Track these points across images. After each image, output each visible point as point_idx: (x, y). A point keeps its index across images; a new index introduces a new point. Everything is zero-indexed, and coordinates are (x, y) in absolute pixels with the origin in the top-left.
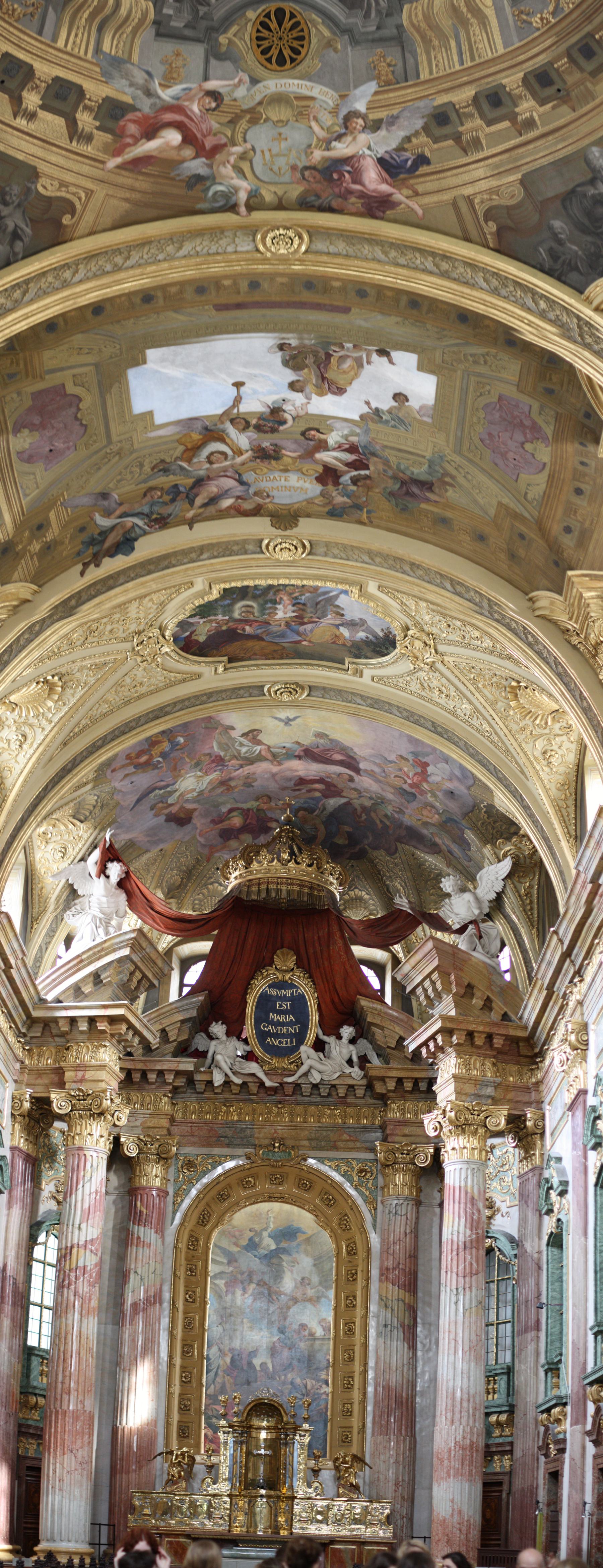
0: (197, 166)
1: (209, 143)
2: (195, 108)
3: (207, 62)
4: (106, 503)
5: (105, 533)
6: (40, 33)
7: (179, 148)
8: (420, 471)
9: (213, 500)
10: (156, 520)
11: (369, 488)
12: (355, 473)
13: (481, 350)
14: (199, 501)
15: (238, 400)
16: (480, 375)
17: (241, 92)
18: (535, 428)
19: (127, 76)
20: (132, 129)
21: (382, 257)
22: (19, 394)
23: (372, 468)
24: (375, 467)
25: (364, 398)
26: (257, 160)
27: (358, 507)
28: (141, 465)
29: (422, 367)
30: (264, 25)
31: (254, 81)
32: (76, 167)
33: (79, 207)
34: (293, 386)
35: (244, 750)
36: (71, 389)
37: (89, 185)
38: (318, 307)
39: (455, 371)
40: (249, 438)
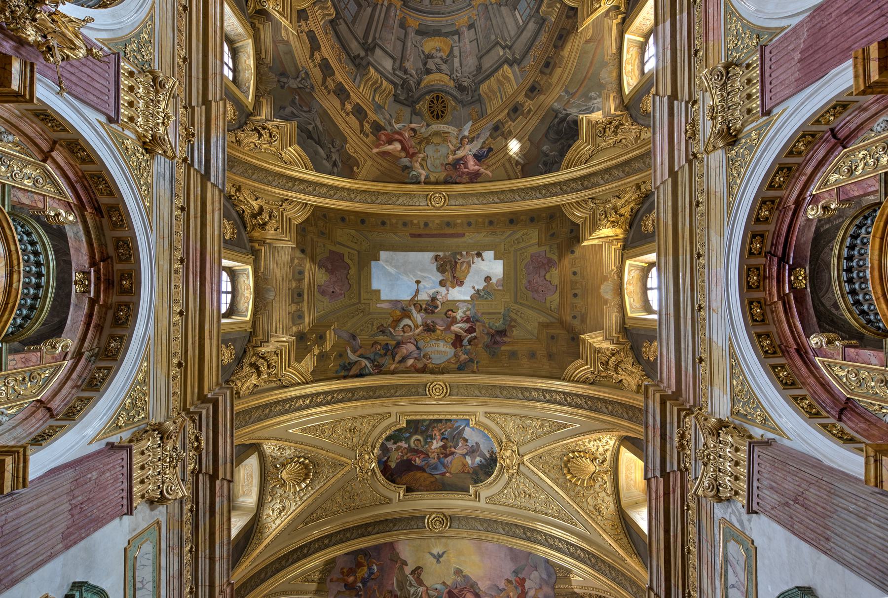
0: (406, 161)
1: (411, 152)
2: (407, 135)
3: (411, 115)
4: (354, 343)
5: (352, 364)
6: (354, 82)
7: (400, 151)
9: (404, 359)
10: (376, 366)
11: (476, 345)
12: (470, 336)
13: (520, 234)
14: (398, 358)
15: (417, 292)
16: (521, 249)
17: (423, 130)
21: (477, 202)
22: (324, 246)
23: (477, 330)
24: (479, 327)
25: (472, 285)
26: (429, 161)
27: (471, 360)
28: (373, 325)
29: (496, 258)
30: (432, 101)
31: (428, 125)
32: (362, 146)
33: (361, 165)
34: (442, 283)
35: (412, 590)
36: (346, 260)
37: (366, 158)
38: (452, 235)
39: (510, 253)
40: (421, 316)
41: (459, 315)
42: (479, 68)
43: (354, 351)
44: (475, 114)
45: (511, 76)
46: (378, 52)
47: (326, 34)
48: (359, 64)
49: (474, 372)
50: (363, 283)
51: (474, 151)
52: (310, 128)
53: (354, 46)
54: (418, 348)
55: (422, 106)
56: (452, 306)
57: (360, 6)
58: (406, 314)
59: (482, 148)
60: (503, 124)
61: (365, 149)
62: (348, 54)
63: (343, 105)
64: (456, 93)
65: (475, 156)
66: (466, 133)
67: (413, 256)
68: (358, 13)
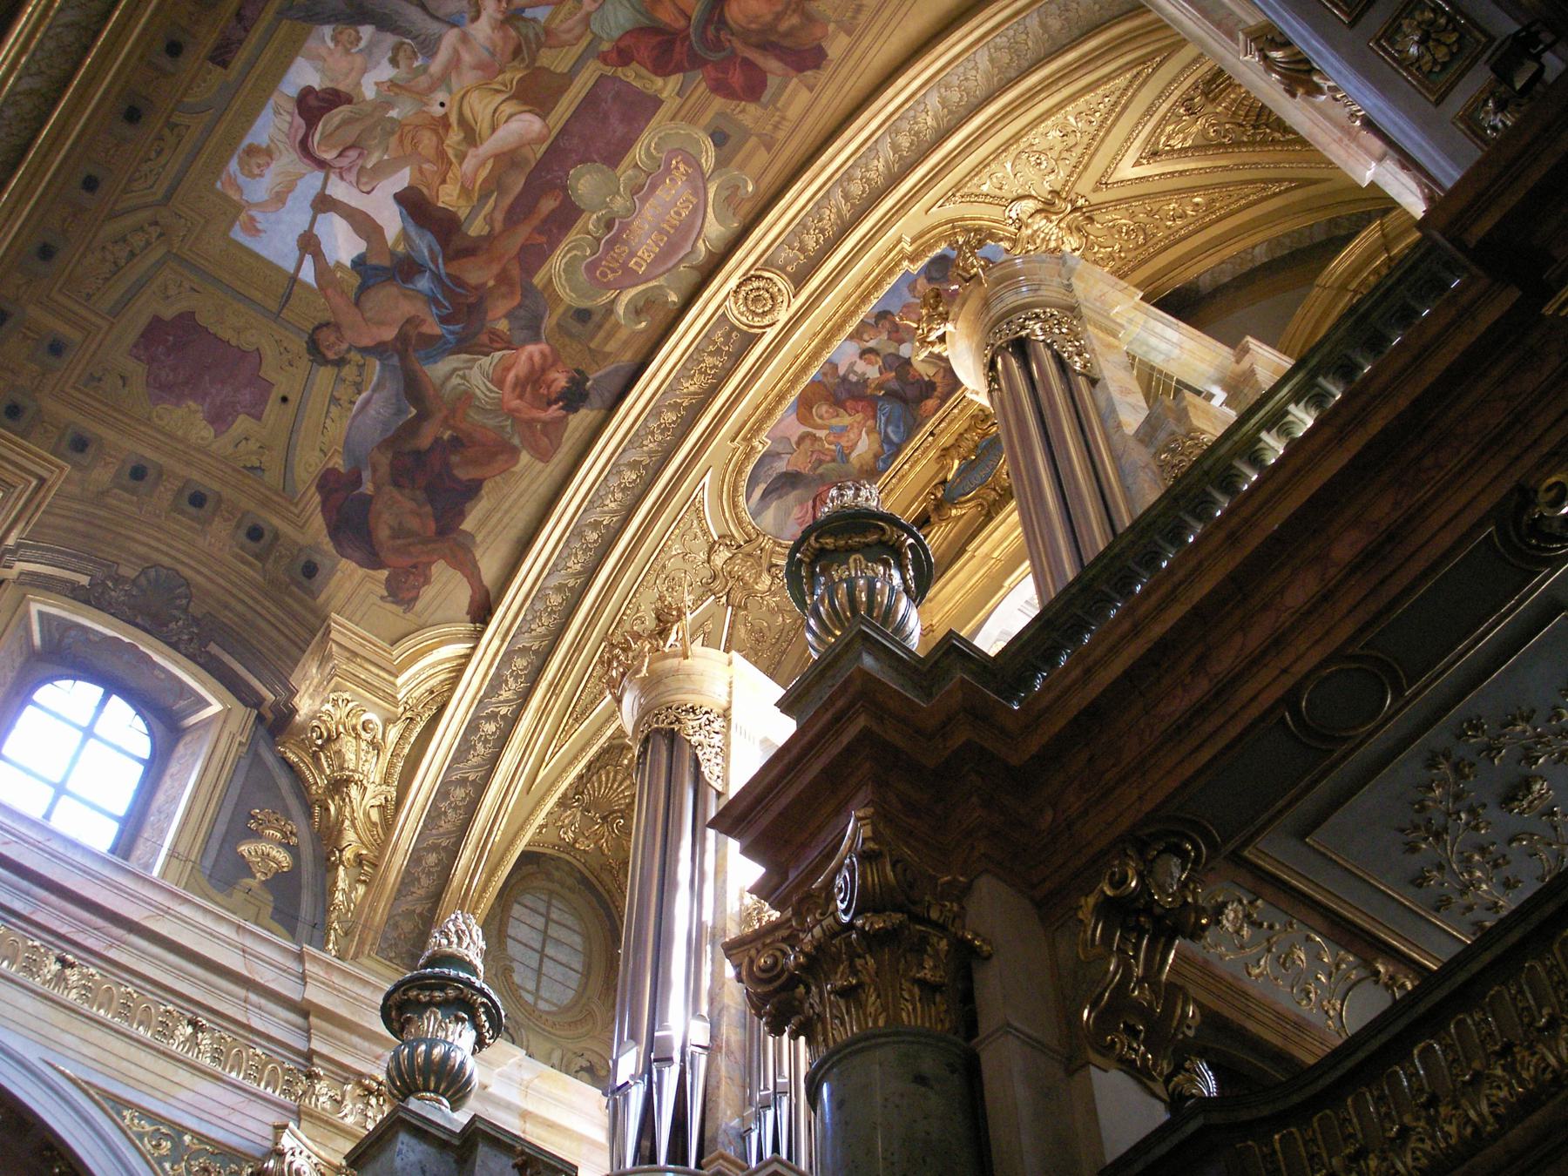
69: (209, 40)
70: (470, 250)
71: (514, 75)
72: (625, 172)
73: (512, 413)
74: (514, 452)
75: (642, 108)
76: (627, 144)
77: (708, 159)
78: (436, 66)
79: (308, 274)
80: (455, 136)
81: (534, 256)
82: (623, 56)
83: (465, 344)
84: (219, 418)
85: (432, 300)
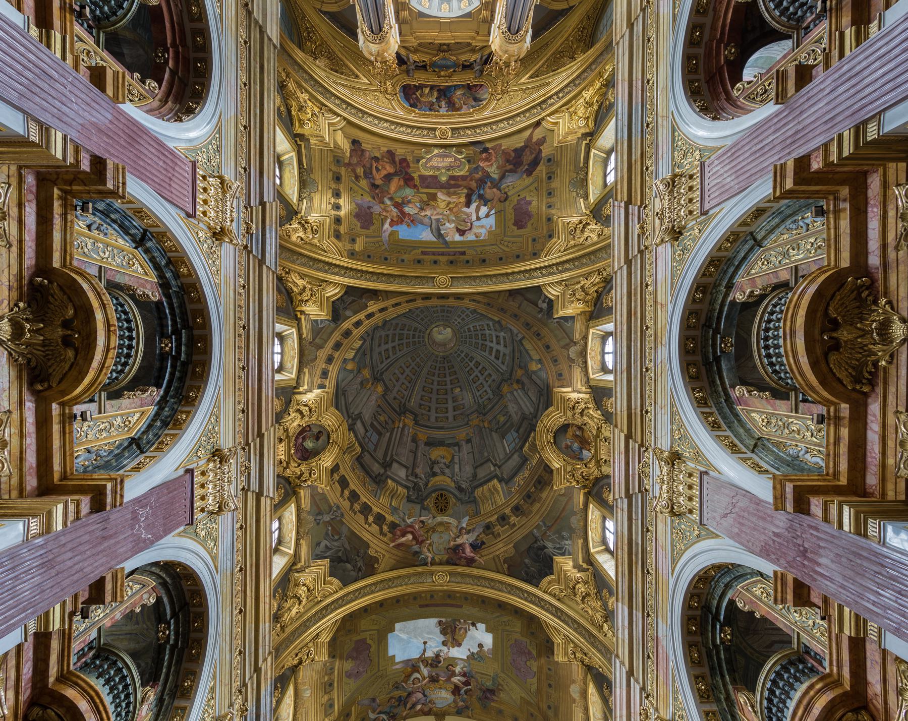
0: (416, 548)
8: (489, 684)
9: (414, 706)
11: (471, 696)
14: (409, 706)
15: (425, 651)
16: (507, 631)
17: (430, 521)
18: (530, 653)
19: (398, 514)
20: (398, 533)
24: (472, 681)
27: (467, 707)
31: (434, 517)
37: (384, 552)
38: (452, 606)
41: (458, 670)
42: (475, 476)
43: (373, 712)
44: (471, 512)
45: (500, 489)
46: (395, 465)
47: (354, 470)
48: (379, 481)
49: (469, 717)
50: (381, 655)
51: (471, 541)
52: (340, 554)
53: (376, 468)
54: (425, 696)
55: (430, 503)
56: (452, 662)
57: (380, 434)
58: (415, 669)
59: (476, 540)
60: (494, 526)
61: (384, 547)
62: (371, 477)
63: (366, 519)
64: (457, 493)
65: (471, 545)
66: (464, 525)
67: (421, 622)
68: (379, 441)
69: (462, 257)
70: (470, 189)
71: (432, 203)
72: (437, 173)
73: (496, 157)
74: (503, 151)
75: (423, 178)
76: (431, 176)
77: (424, 160)
78: (440, 217)
79: (493, 212)
80: (451, 206)
81: (463, 178)
82: (415, 186)
83: (487, 175)
84: (530, 203)
85: (484, 188)
